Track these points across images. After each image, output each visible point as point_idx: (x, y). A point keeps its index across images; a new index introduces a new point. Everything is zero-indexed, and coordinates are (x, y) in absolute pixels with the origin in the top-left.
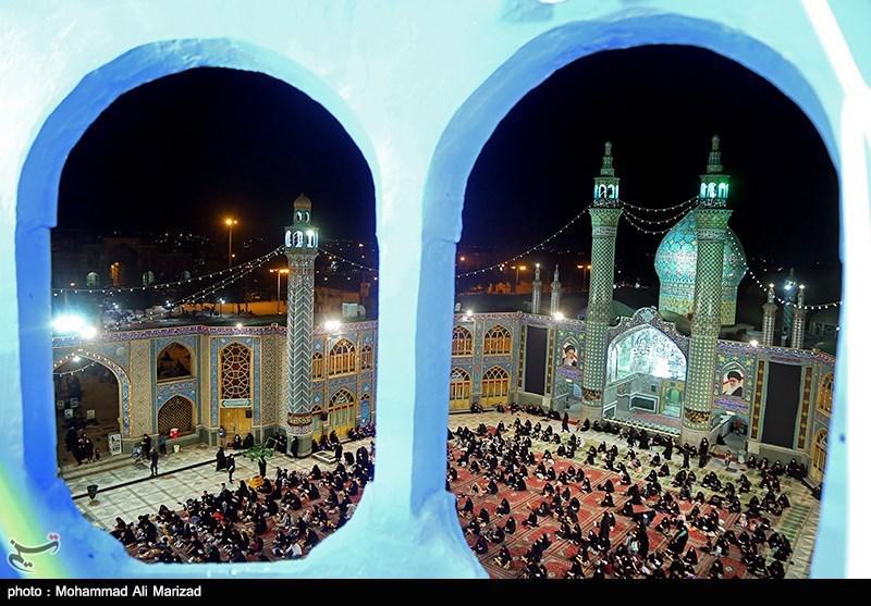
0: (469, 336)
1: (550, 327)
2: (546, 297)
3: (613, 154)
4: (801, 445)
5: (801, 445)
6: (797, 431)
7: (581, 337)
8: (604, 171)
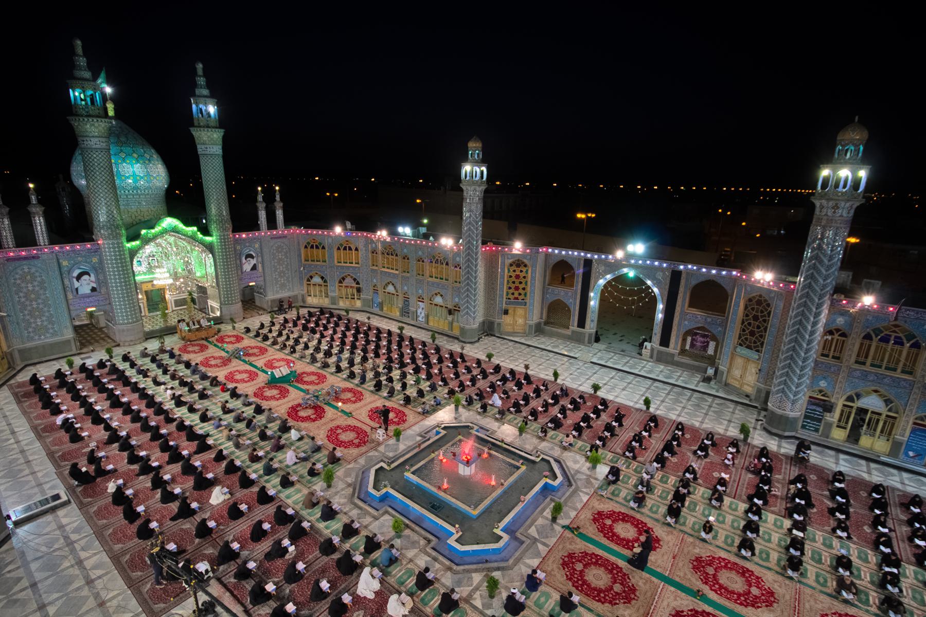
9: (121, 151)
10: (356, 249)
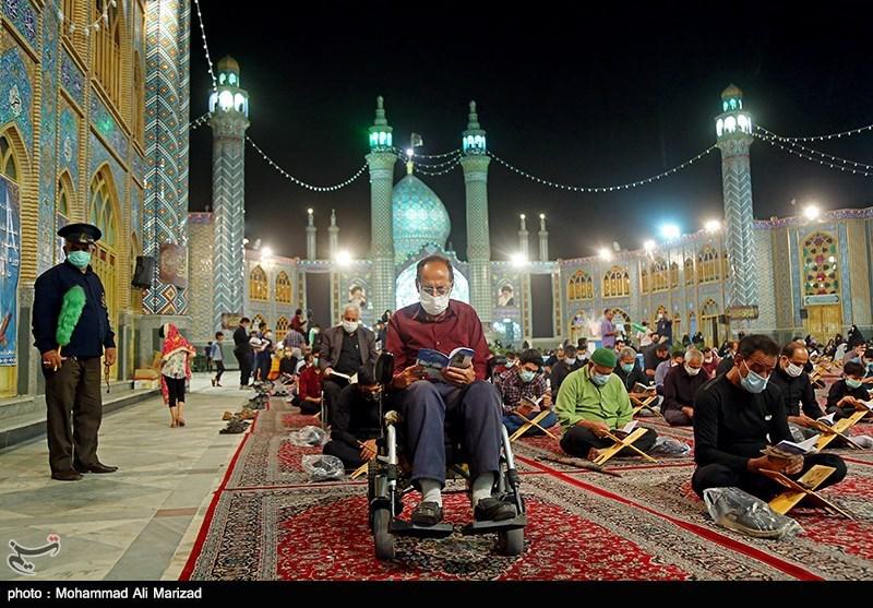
0: (265, 280)
1: (332, 270)
2: (322, 236)
3: (385, 107)
4: (559, 334)
5: (559, 334)
6: (555, 323)
7: (367, 277)
8: (377, 122)
9: (410, 199)
10: (626, 275)
